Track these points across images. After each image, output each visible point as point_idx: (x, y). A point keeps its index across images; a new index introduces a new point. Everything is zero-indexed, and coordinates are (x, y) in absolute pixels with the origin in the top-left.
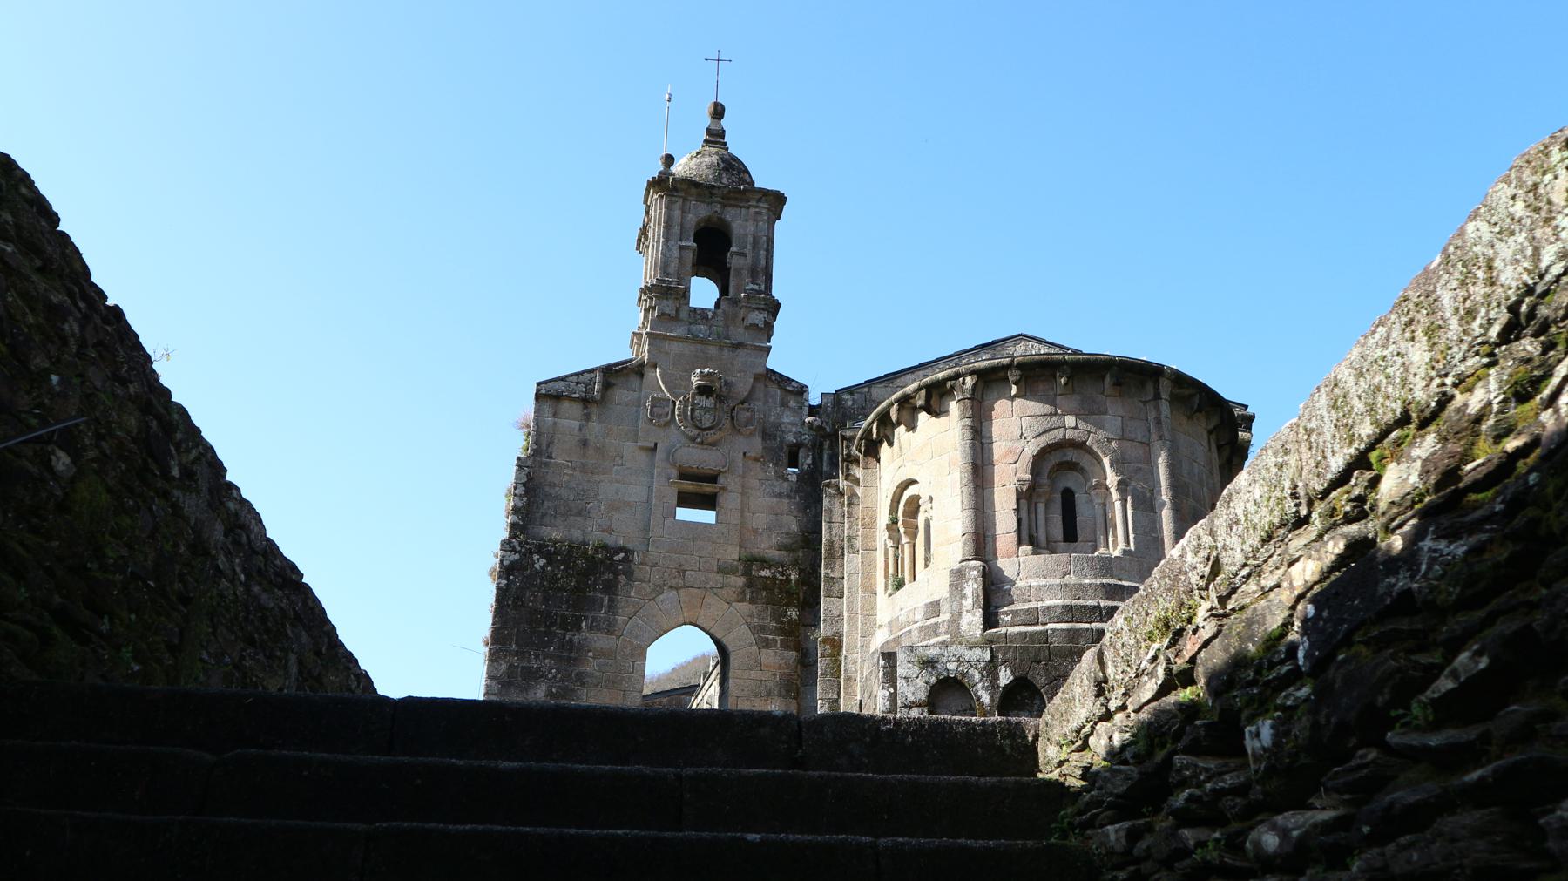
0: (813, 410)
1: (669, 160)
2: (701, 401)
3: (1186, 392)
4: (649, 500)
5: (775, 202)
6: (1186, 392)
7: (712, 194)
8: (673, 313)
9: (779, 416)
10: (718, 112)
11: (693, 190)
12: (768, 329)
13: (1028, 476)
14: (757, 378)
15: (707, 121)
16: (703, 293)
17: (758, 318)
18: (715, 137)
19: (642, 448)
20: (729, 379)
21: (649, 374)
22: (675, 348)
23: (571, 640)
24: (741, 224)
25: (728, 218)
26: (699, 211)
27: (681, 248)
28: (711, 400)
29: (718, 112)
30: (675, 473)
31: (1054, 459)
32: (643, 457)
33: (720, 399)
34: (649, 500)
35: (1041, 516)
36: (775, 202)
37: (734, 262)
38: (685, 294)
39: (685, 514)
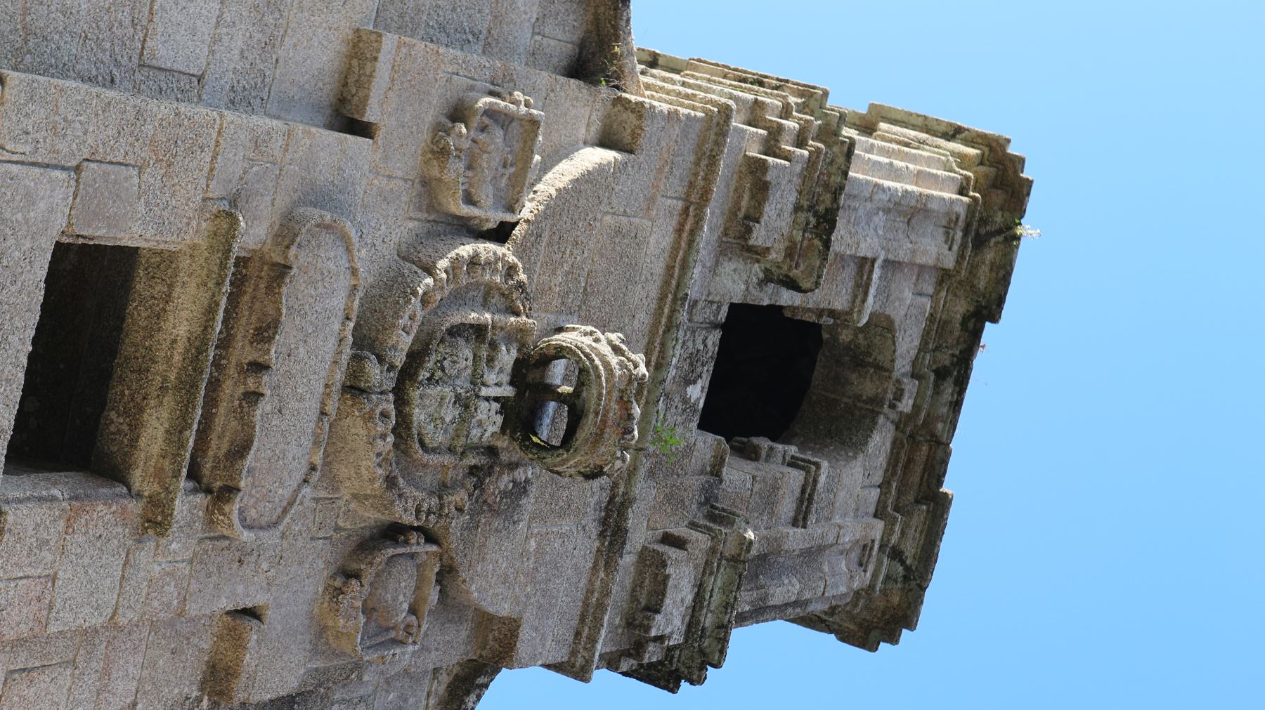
4: (148, 75)
7: (941, 374)
11: (961, 307)
19: (360, 52)
20: (528, 504)
21: (582, 105)
22: (658, 238)
30: (253, 234)
32: (313, 55)
34: (148, 75)
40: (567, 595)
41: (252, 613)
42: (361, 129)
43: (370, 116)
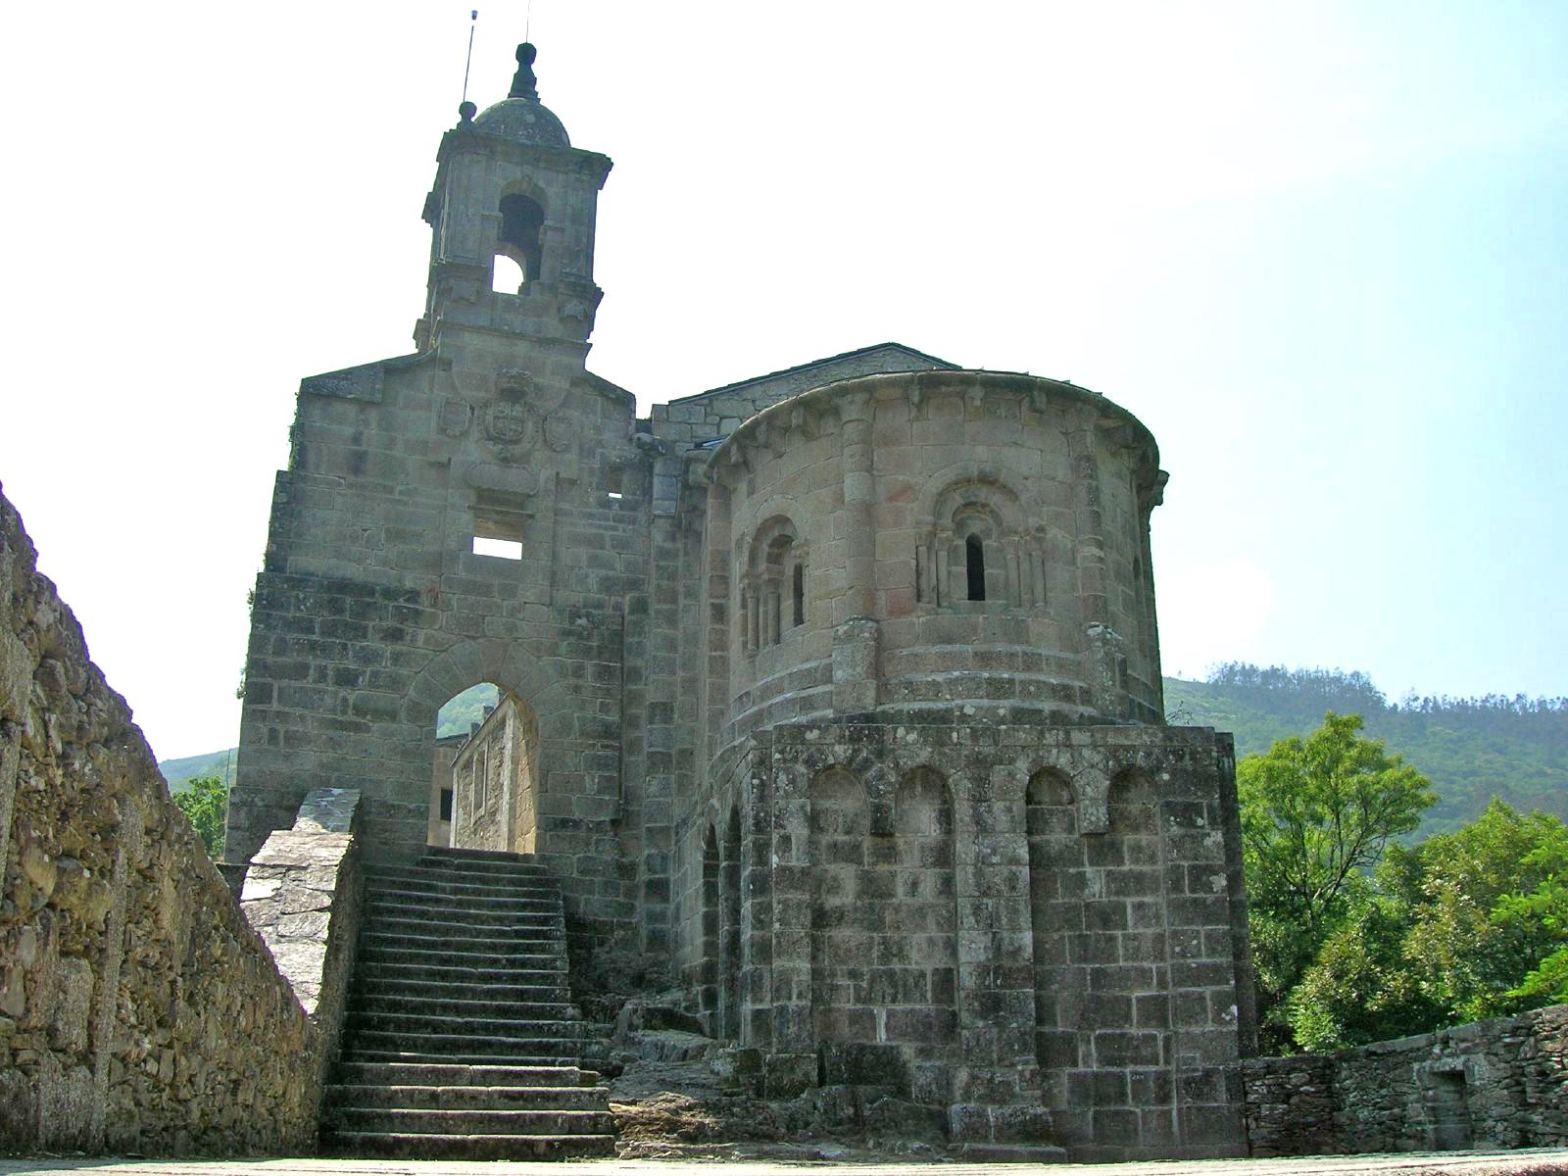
0: (645, 426)
2: (506, 408)
3: (1109, 423)
5: (597, 167)
6: (1109, 423)
8: (473, 299)
9: (598, 430)
10: (526, 54)
13: (930, 518)
14: (574, 383)
15: (514, 66)
16: (508, 275)
17: (573, 307)
18: (524, 82)
23: (345, 700)
25: (542, 184)
27: (484, 218)
28: (518, 407)
29: (526, 54)
30: (473, 498)
31: (958, 500)
33: (531, 409)
35: (943, 568)
36: (597, 167)
37: (549, 239)
38: (487, 275)
39: (484, 546)
40: (566, 360)
41: (558, 474)
42: (450, 460)
43: (444, 460)
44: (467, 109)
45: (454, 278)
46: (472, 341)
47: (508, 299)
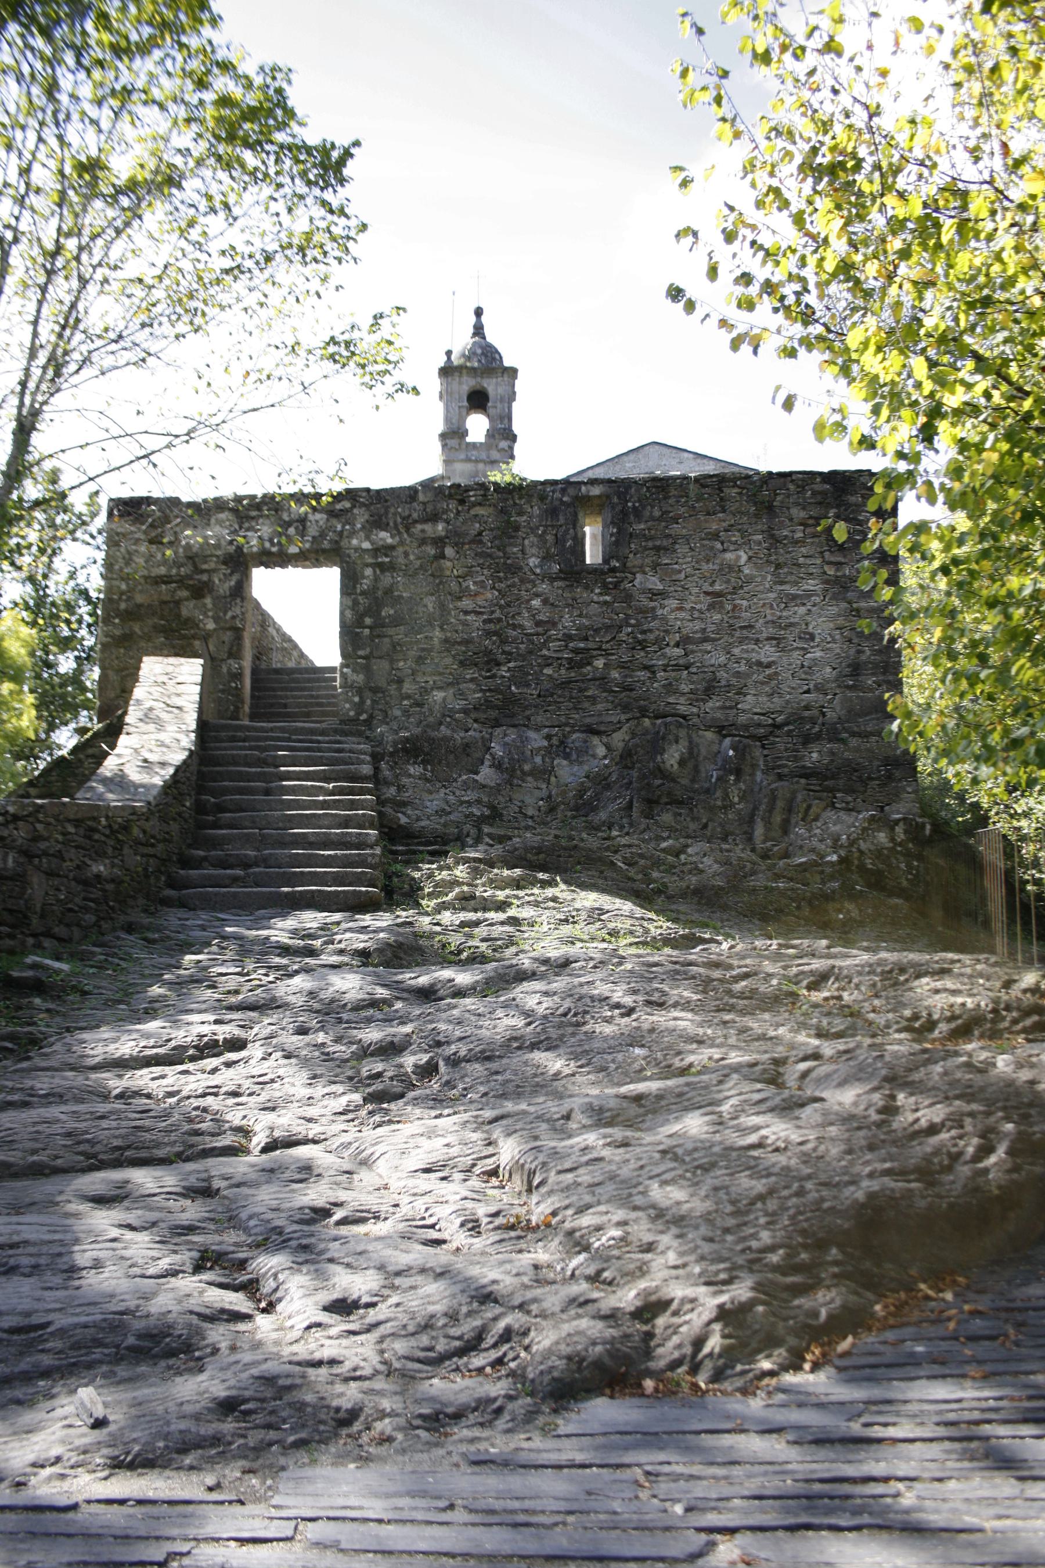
1: (449, 353)
5: (513, 372)
10: (479, 312)
12: (511, 448)
15: (473, 319)
17: (503, 444)
18: (479, 330)
24: (492, 386)
26: (467, 384)
29: (479, 312)
36: (513, 372)
44: (449, 353)
45: (453, 436)
46: (459, 467)
47: (474, 445)
